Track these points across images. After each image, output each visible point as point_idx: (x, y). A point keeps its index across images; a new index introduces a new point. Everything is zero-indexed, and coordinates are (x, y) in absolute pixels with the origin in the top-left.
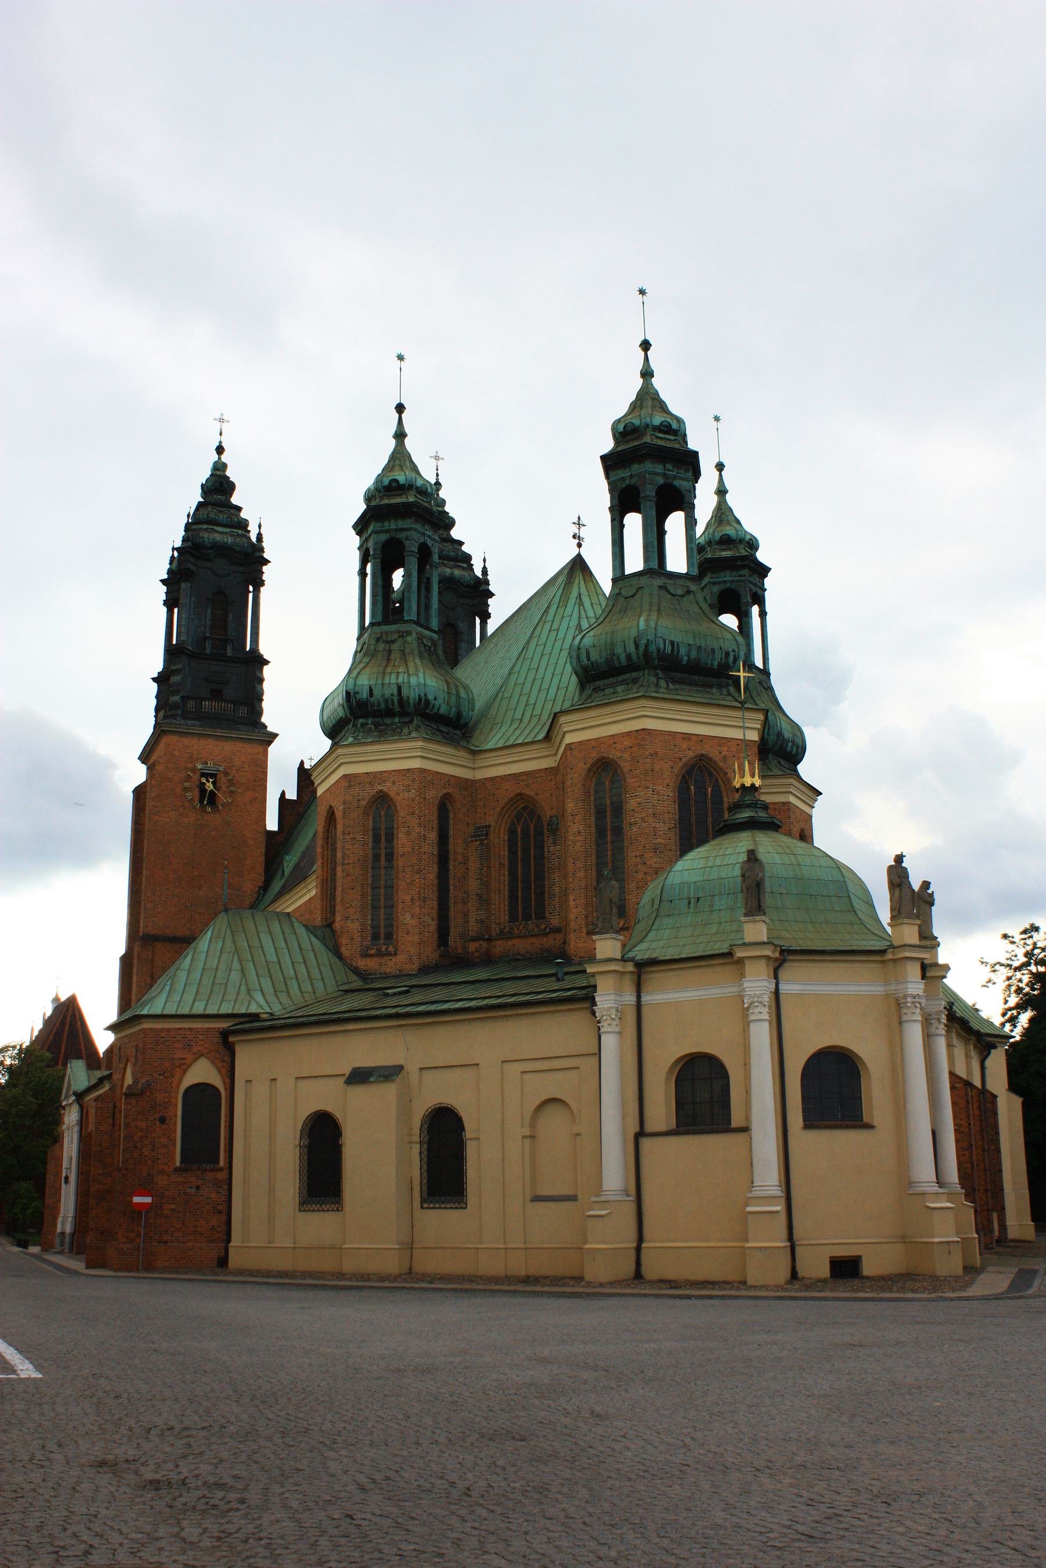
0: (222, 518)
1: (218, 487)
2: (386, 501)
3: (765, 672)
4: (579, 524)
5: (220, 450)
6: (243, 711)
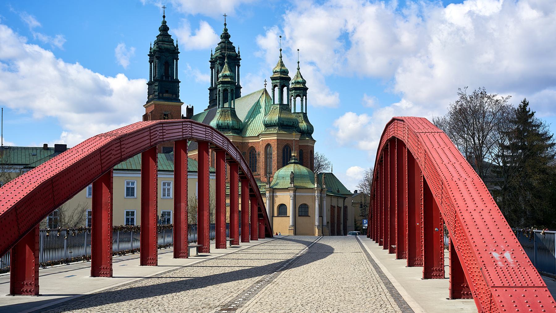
0: (166, 39)
1: (164, 29)
2: (224, 80)
3: (306, 113)
4: (265, 81)
5: (164, 17)
6: (174, 96)
